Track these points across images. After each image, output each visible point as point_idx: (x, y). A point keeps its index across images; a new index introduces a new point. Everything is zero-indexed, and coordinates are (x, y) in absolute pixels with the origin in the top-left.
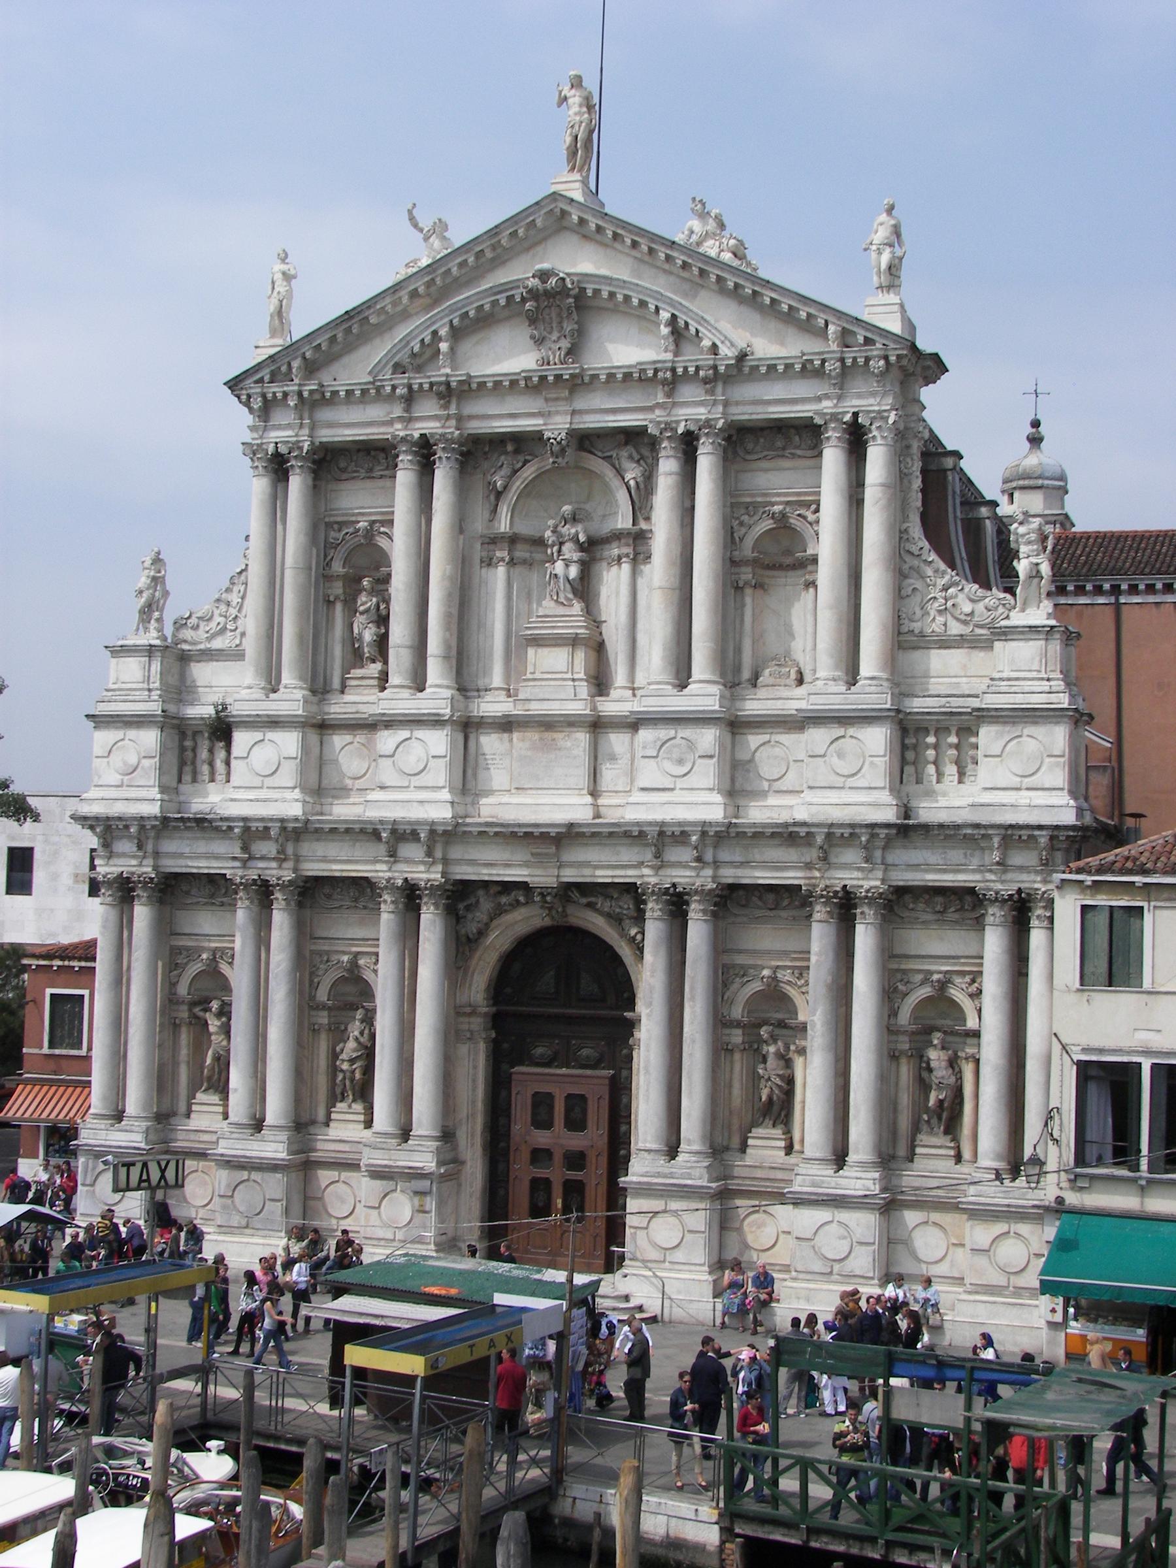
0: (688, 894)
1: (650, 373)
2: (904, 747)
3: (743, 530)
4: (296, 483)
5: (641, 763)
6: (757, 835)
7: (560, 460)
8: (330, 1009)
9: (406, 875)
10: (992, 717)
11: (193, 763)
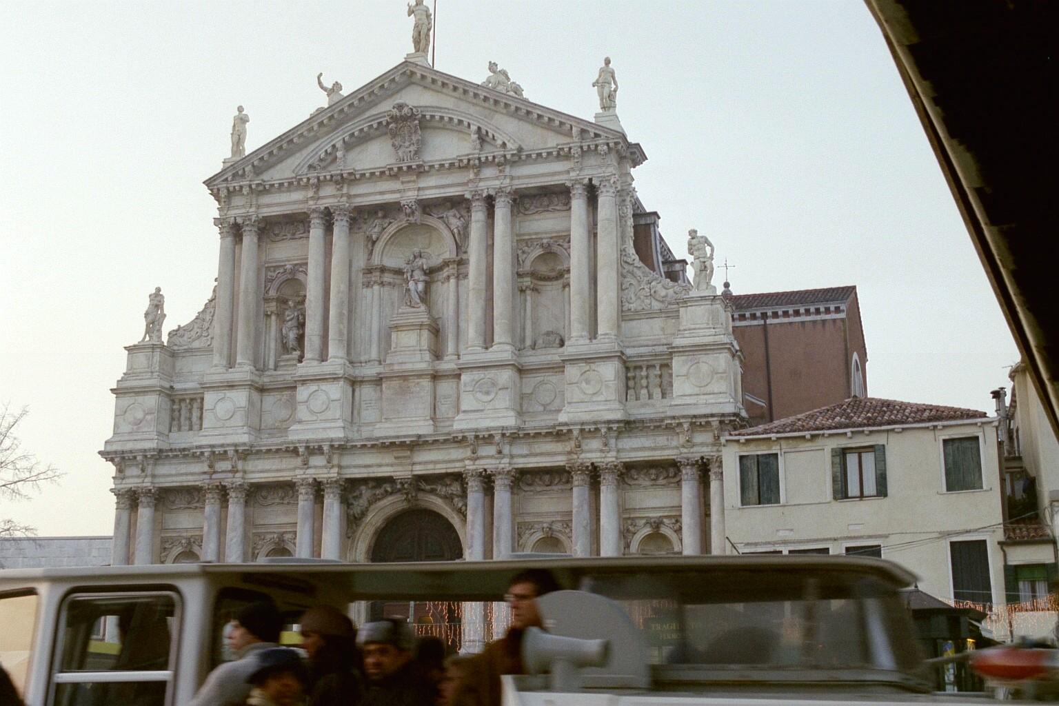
0: (494, 475)
1: (465, 162)
2: (628, 379)
3: (525, 256)
4: (249, 240)
5: (463, 396)
6: (538, 435)
7: (411, 218)
9: (314, 476)
10: (680, 352)
11: (179, 420)
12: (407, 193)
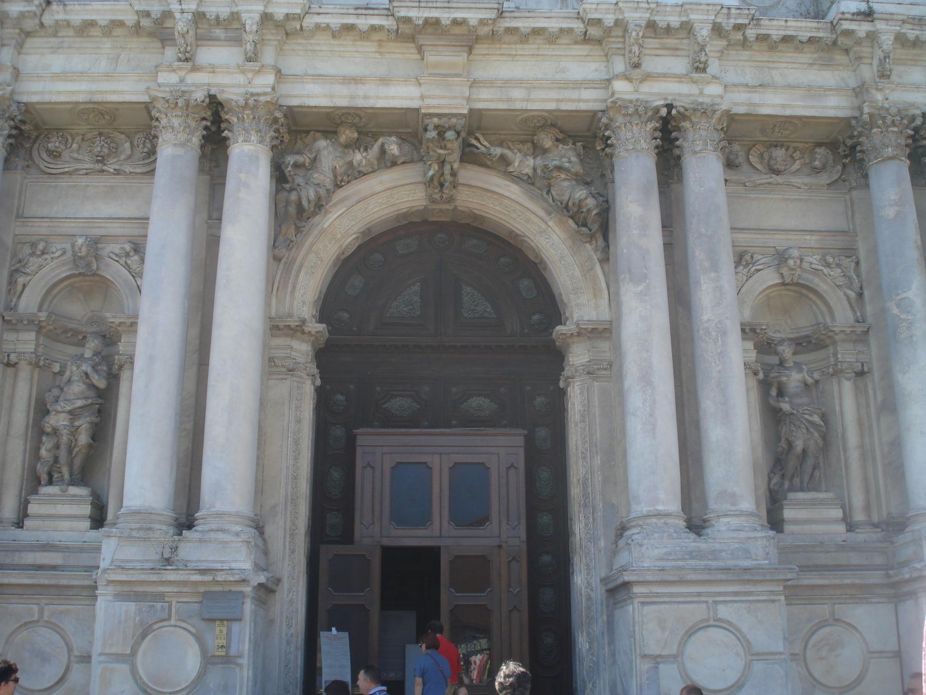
8: (39, 329)
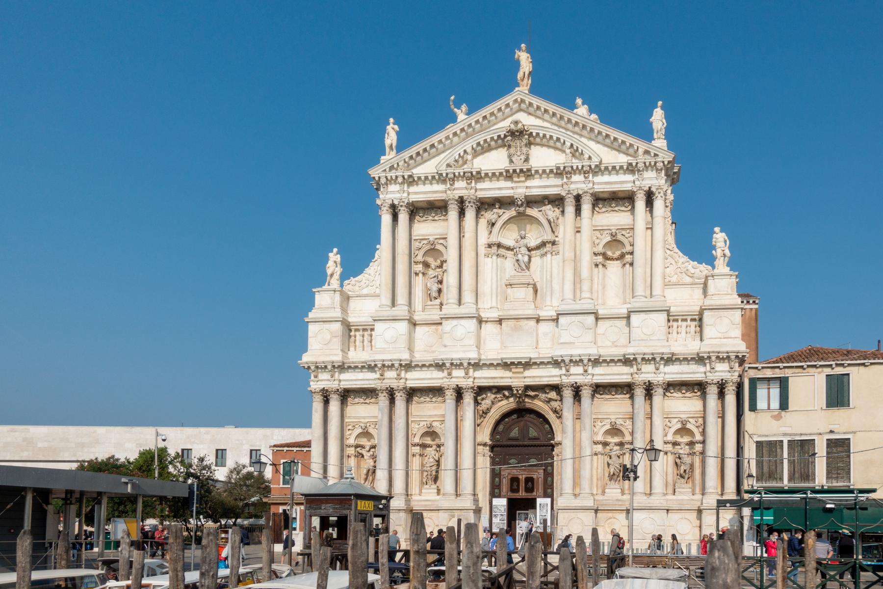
12: (519, 189)
